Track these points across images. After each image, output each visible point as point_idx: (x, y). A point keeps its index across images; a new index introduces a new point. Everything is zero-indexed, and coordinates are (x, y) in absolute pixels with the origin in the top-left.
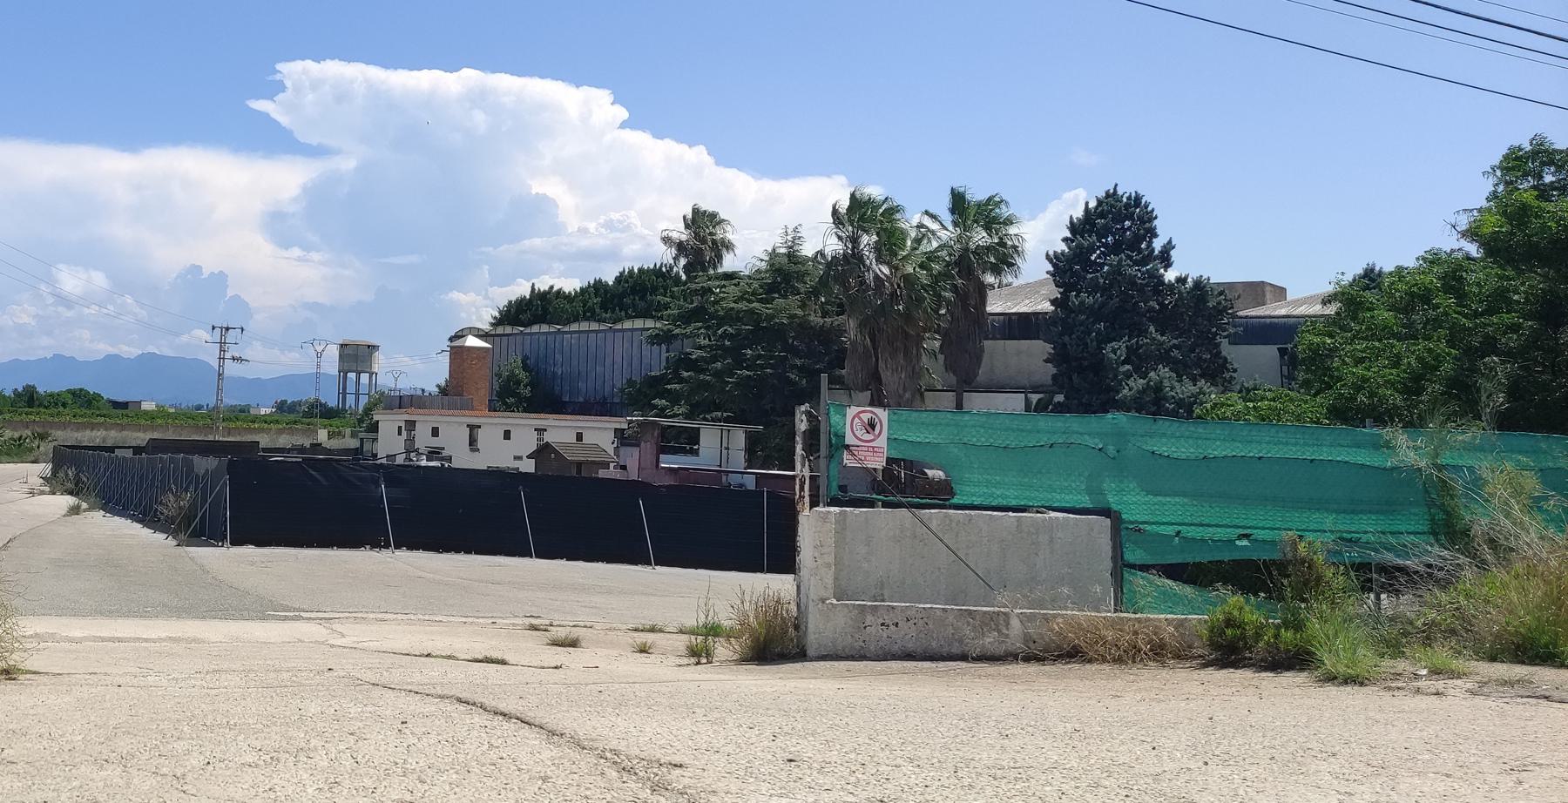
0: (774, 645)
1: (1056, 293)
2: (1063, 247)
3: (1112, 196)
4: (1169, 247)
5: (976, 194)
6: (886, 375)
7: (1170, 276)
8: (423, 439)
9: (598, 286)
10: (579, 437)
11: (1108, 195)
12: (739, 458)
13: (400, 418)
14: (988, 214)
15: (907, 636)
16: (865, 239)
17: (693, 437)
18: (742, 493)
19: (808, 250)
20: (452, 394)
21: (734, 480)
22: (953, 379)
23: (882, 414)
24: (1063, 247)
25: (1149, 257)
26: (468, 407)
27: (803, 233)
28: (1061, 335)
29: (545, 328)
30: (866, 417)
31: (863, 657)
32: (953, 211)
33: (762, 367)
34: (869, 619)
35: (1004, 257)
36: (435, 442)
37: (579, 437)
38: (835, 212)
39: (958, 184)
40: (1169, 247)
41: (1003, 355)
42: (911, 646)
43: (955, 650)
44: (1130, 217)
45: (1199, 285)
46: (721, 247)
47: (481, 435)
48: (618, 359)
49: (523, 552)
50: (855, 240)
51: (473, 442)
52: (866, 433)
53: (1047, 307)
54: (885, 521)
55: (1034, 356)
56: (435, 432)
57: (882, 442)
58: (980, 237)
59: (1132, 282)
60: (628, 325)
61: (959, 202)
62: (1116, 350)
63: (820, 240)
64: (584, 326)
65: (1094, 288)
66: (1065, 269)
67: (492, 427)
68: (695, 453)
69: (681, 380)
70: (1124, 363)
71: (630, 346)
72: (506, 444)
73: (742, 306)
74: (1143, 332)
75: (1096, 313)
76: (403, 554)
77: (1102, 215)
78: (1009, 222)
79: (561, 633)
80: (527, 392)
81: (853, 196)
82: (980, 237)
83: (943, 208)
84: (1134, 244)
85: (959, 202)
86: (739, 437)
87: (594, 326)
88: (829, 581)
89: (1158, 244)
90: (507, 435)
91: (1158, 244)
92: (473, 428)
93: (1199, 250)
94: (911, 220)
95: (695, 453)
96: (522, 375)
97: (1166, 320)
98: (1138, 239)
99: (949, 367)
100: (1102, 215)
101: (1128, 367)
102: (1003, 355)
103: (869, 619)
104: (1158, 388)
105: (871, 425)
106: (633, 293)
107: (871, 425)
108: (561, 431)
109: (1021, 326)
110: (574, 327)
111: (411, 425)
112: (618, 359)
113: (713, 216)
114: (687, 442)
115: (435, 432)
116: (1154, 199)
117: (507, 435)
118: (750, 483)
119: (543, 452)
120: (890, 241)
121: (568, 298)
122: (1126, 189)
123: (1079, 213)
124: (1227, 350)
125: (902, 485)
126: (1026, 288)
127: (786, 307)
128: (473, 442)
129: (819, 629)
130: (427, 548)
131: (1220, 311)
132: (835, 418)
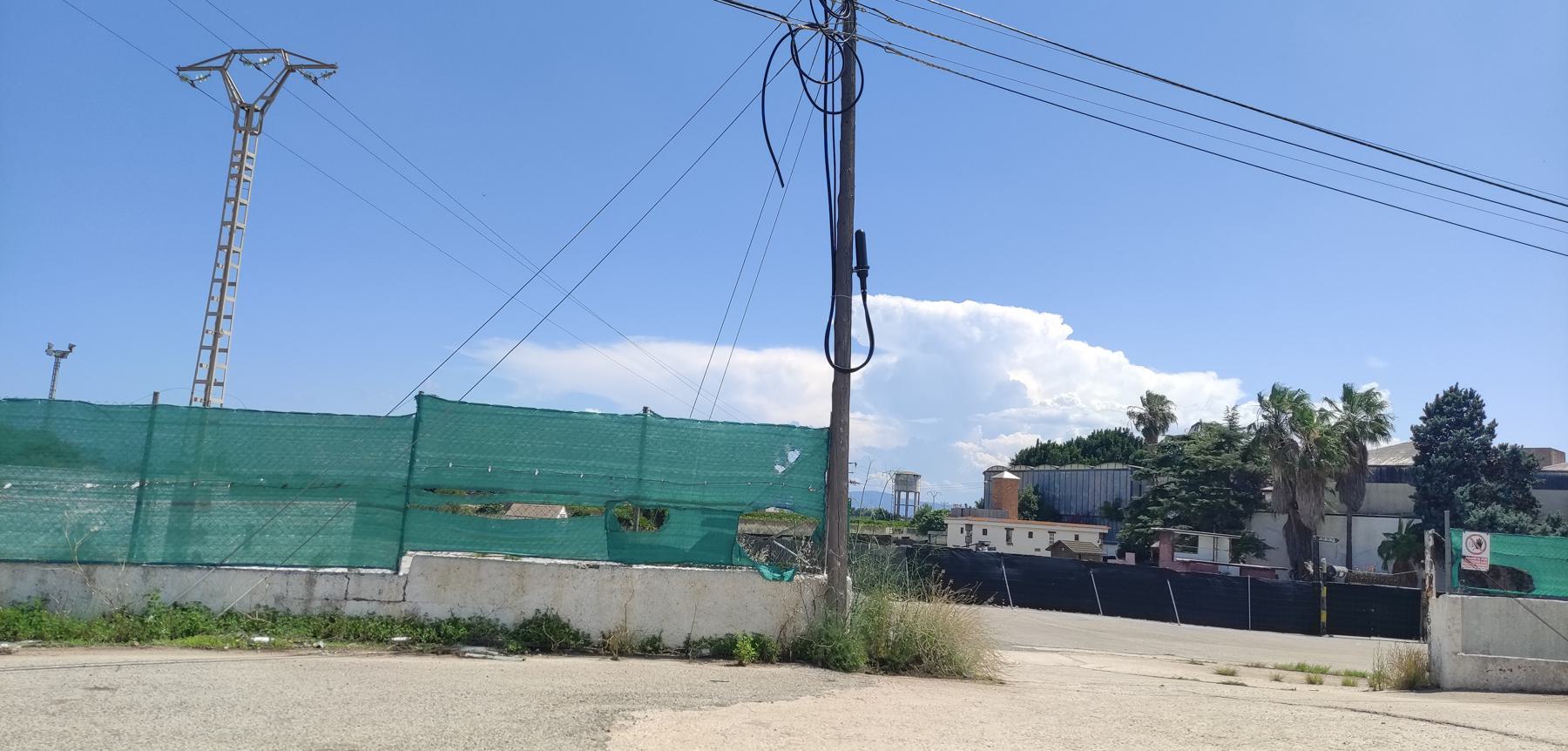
0: (1420, 681)
1: (1417, 453)
2: (1420, 423)
3: (1454, 390)
4: (1494, 424)
6: (1301, 503)
7: (1495, 443)
8: (977, 536)
9: (1079, 441)
10: (1077, 538)
11: (1452, 390)
12: (1225, 555)
13: (962, 522)
14: (1368, 402)
15: (1519, 677)
16: (1283, 417)
17: (1195, 542)
18: (1225, 578)
19: (1243, 422)
20: (991, 504)
21: (1222, 569)
22: (1344, 508)
23: (1486, 537)
24: (1420, 423)
25: (1481, 431)
26: (1005, 516)
28: (1424, 481)
29: (1048, 467)
30: (1475, 539)
31: (1487, 690)
32: (1344, 399)
33: (1216, 497)
34: (1490, 666)
35: (1380, 429)
36: (984, 538)
37: (1077, 538)
38: (1260, 399)
40: (1494, 424)
41: (1377, 493)
42: (1522, 684)
43: (1556, 687)
44: (1467, 405)
45: (1515, 450)
46: (1168, 418)
47: (1014, 534)
49: (1093, 610)
50: (1277, 417)
51: (1008, 538)
52: (1477, 549)
53: (1409, 461)
54: (1491, 605)
55: (1403, 494)
56: (985, 532)
57: (1486, 555)
58: (1361, 416)
59: (1470, 448)
60: (1104, 466)
61: (1348, 394)
63: (1251, 416)
64: (1075, 467)
65: (1443, 452)
66: (1425, 439)
67: (1021, 529)
68: (1195, 551)
69: (1159, 504)
71: (1113, 480)
72: (1033, 540)
73: (1201, 457)
74: (1478, 480)
75: (1447, 468)
76: (1017, 610)
77: (1448, 404)
78: (1381, 406)
79: (1223, 666)
80: (1036, 507)
82: (1361, 416)
83: (1337, 396)
84: (1470, 423)
85: (1348, 394)
86: (1225, 542)
87: (1081, 467)
88: (1459, 641)
89: (1486, 423)
90: (1031, 535)
91: (1486, 423)
92: (1008, 530)
93: (1514, 425)
94: (1317, 405)
95: (1195, 551)
96: (1034, 497)
97: (1493, 472)
98: (1472, 419)
99: (1343, 500)
100: (1448, 404)
102: (1377, 493)
103: (1490, 666)
105: (1479, 544)
106: (1102, 447)
107: (1479, 544)
108: (1065, 533)
109: (1390, 474)
110: (1068, 467)
111: (969, 527)
113: (1162, 398)
114: (1192, 545)
115: (985, 532)
116: (1483, 394)
117: (1031, 535)
118: (1234, 571)
119: (1056, 547)
120: (1303, 417)
121: (1061, 448)
123: (1432, 400)
124: (1535, 493)
125: (1514, 581)
126: (1394, 447)
127: (1229, 459)
128: (1008, 538)
129: (1450, 670)
130: (1032, 607)
131: (1530, 467)
132: (1455, 539)
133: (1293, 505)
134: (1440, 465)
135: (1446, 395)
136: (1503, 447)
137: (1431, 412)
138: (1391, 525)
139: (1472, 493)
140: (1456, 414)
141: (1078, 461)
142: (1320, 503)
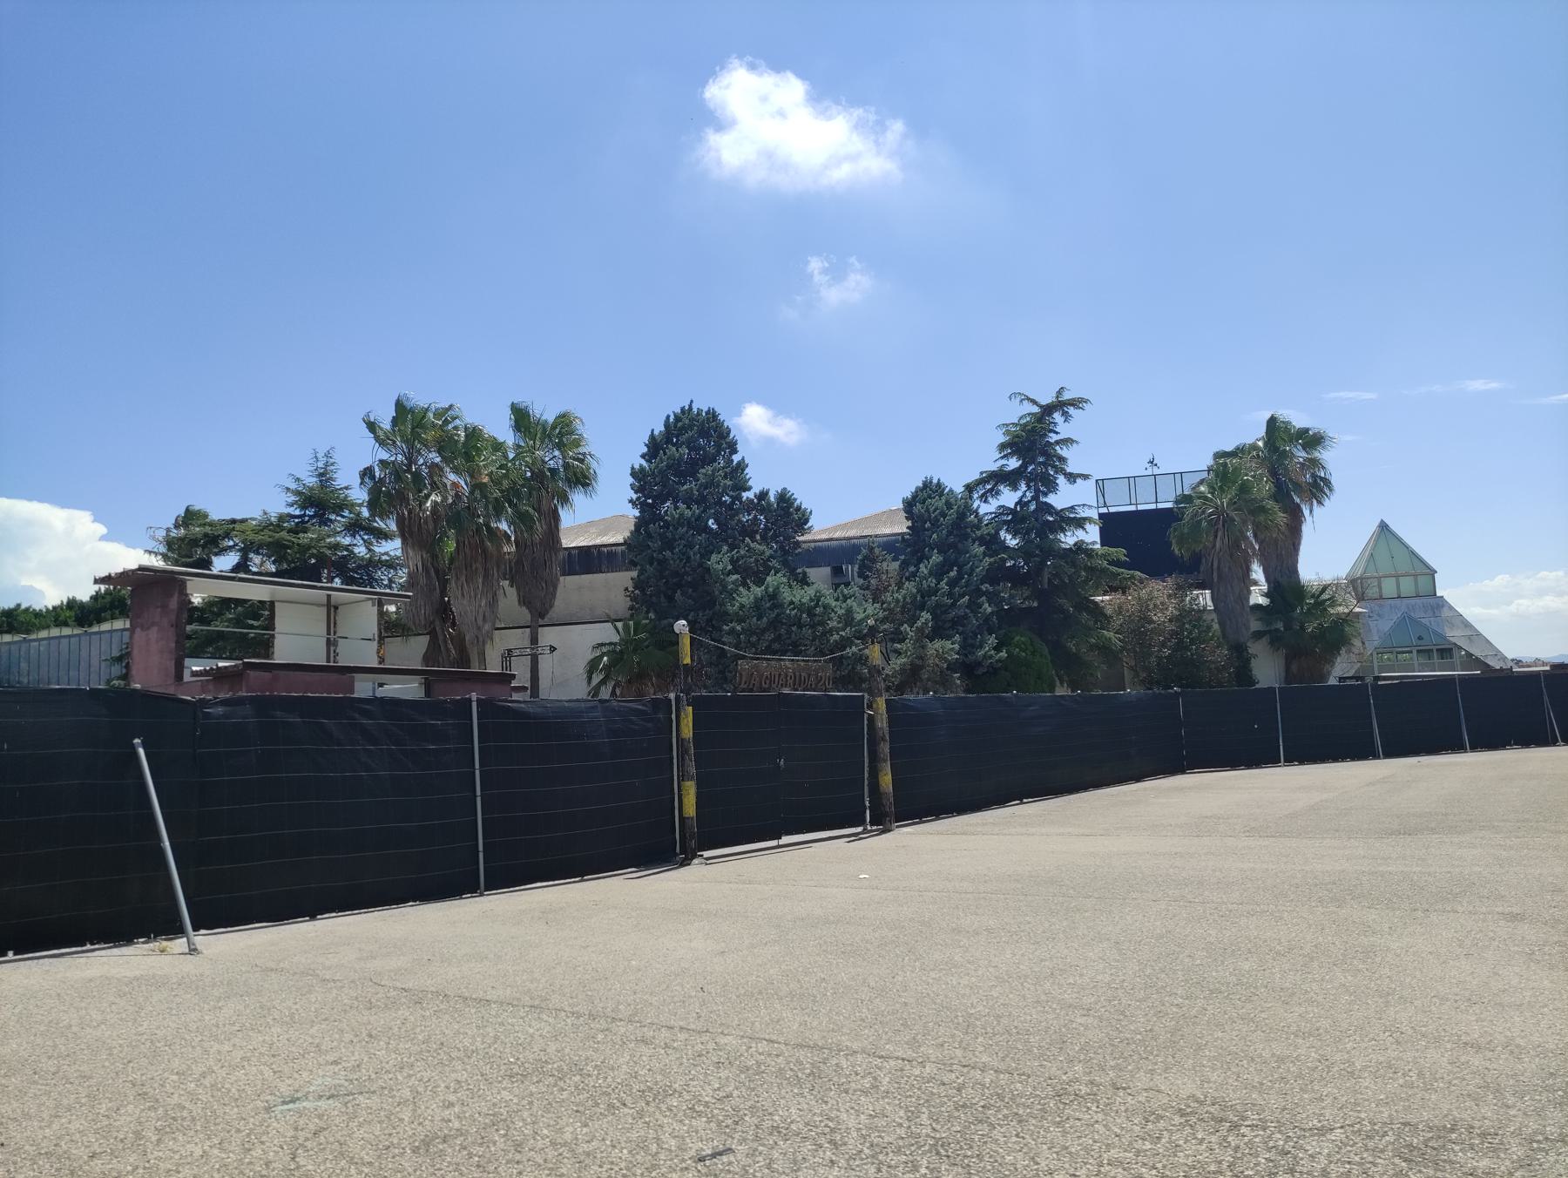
5: (545, 410)
9: (72, 604)
14: (562, 432)
22: (524, 615)
27: (337, 457)
38: (372, 426)
39: (521, 398)
48: (95, 662)
55: (614, 587)
60: (106, 627)
61: (521, 418)
62: (719, 562)
64: (55, 632)
70: (730, 573)
77: (684, 429)
81: (400, 406)
82: (552, 458)
85: (521, 418)
89: (736, 458)
99: (524, 601)
101: (735, 577)
102: (573, 590)
104: (774, 596)
109: (590, 560)
112: (95, 662)
122: (702, 405)
123: (659, 428)
126: (600, 514)
133: (444, 612)
134: (681, 521)
135: (677, 419)
136: (763, 495)
137: (655, 447)
138: (607, 633)
139: (732, 561)
140: (691, 452)
141: (66, 624)
142: (493, 603)
